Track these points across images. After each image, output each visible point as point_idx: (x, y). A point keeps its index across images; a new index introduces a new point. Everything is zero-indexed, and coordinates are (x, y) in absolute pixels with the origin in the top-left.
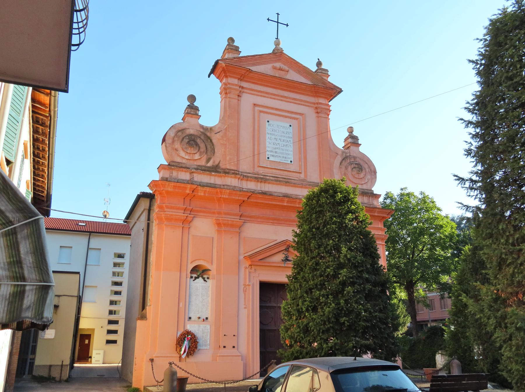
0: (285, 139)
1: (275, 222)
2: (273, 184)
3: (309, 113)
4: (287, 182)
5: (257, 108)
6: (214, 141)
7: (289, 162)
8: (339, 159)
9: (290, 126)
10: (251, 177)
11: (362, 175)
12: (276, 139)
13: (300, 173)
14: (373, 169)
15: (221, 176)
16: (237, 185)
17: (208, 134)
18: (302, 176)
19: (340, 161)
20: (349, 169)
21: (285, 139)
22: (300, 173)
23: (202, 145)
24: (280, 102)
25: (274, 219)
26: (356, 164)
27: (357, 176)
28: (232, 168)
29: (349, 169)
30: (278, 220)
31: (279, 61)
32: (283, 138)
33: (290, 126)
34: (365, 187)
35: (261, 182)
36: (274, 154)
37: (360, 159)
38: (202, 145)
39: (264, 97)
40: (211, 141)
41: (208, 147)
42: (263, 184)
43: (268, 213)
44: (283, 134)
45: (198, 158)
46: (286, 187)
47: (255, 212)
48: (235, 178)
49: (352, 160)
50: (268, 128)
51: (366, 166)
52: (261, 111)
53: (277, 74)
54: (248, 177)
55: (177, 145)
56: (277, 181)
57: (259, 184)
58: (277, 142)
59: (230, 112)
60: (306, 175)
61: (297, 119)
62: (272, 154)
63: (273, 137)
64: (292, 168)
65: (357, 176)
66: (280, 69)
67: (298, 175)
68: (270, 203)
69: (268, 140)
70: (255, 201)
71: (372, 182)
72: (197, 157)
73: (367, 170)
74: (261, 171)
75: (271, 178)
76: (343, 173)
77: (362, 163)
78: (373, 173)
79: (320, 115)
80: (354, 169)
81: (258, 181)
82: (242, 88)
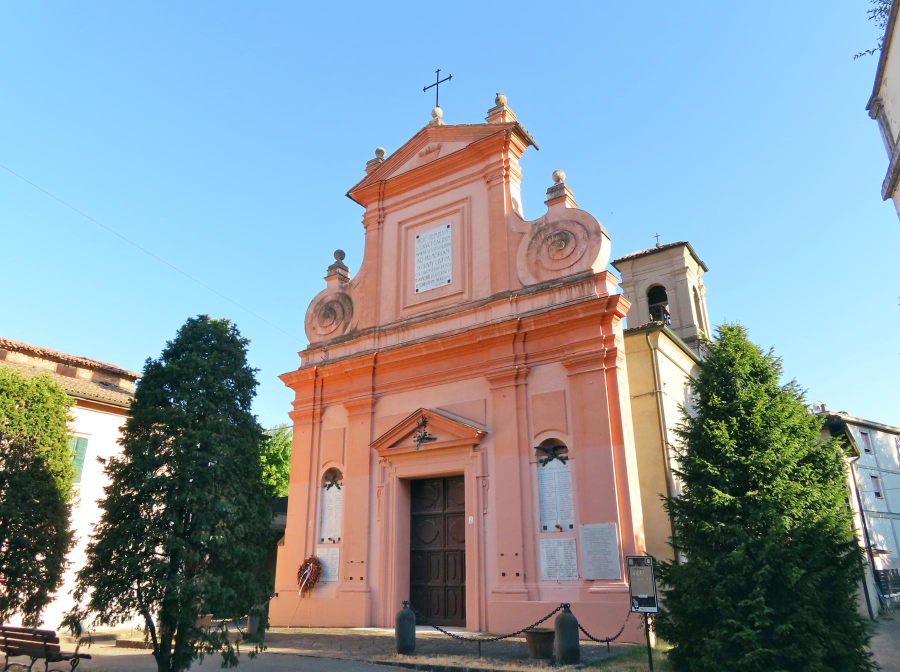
0: (440, 250)
1: (419, 384)
2: (419, 327)
3: (477, 191)
4: (438, 317)
5: (404, 226)
6: (353, 299)
7: (447, 283)
8: (527, 239)
9: (448, 226)
10: (389, 329)
11: (569, 250)
12: (428, 257)
13: (462, 293)
14: (592, 228)
15: (355, 343)
16: (371, 347)
17: (347, 292)
18: (466, 296)
19: (527, 244)
20: (544, 249)
21: (440, 250)
22: (462, 293)
23: (339, 310)
24: (424, 202)
25: (417, 380)
26: (555, 236)
27: (558, 257)
28: (370, 325)
29: (544, 249)
30: (422, 379)
31: (427, 141)
32: (437, 251)
33: (448, 226)
34: (576, 269)
35: (403, 331)
36: (426, 281)
37: (566, 222)
38: (339, 310)
39: (412, 204)
40: (350, 299)
41: (346, 309)
42: (406, 333)
43: (410, 373)
44: (438, 245)
45: (337, 330)
46: (438, 325)
47: (393, 377)
48: (369, 338)
49: (550, 231)
50: (418, 246)
51: (578, 230)
52: (407, 228)
53: (432, 157)
54: (385, 330)
55: (316, 323)
56: (425, 320)
57: (401, 334)
58: (429, 261)
59: (374, 248)
60: (470, 295)
61: (455, 212)
62: (422, 282)
63: (424, 256)
64: (452, 290)
65: (558, 257)
66: (428, 152)
67: (460, 297)
68: (405, 358)
69: (417, 264)
70: (386, 362)
71: (590, 254)
72: (333, 327)
73: (580, 236)
74: (405, 314)
75: (417, 319)
76: (533, 261)
77: (568, 227)
78: (593, 237)
79: (493, 183)
80: (552, 247)
81: (399, 332)
82: (383, 209)
